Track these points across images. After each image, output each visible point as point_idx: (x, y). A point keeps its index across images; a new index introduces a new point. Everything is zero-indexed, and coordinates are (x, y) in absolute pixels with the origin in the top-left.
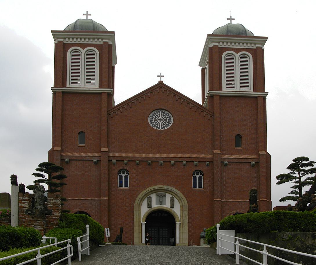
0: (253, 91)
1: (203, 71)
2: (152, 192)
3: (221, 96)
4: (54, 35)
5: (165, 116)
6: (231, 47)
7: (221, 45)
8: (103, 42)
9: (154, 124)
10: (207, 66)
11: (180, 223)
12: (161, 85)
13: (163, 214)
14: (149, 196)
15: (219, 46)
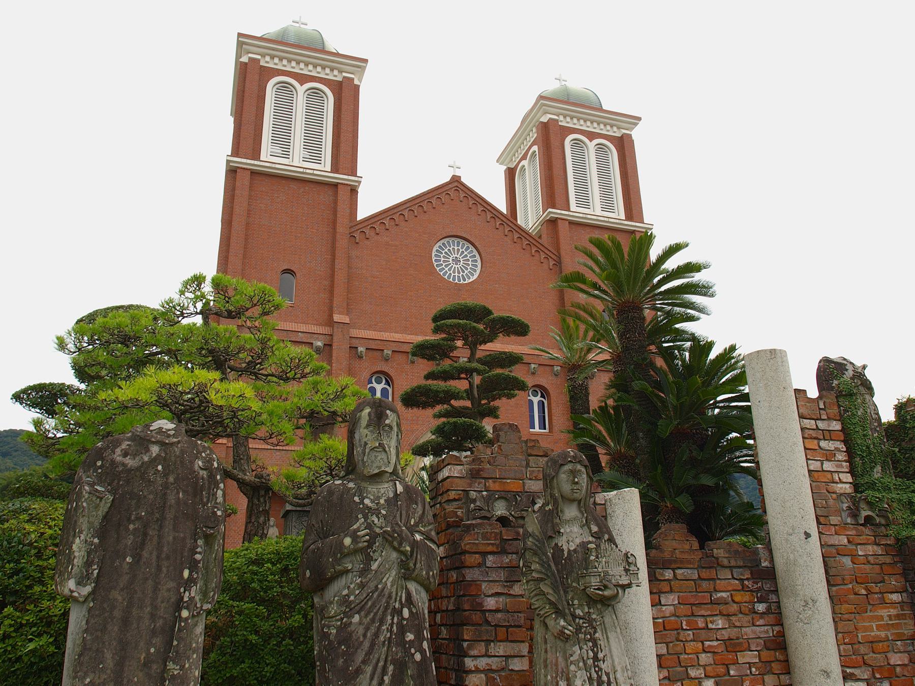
12: (456, 184)
15: (560, 124)
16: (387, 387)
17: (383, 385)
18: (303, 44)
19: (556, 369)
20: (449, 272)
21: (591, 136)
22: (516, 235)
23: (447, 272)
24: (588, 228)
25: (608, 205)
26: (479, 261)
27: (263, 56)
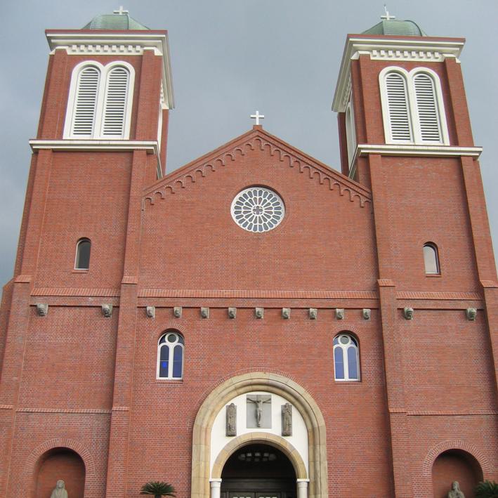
0: (449, 145)
1: (342, 118)
2: (238, 390)
3: (384, 156)
4: (49, 39)
5: (268, 201)
6: (394, 59)
7: (375, 56)
8: (145, 51)
9: (244, 220)
10: (350, 105)
11: (308, 480)
12: (257, 133)
13: (266, 455)
14: (229, 404)
15: (372, 58)
16: (180, 344)
17: (176, 343)
18: (109, 28)
19: (364, 312)
20: (250, 223)
21: (409, 66)
22: (323, 177)
23: (247, 223)
24: (406, 159)
25: (430, 132)
26: (283, 207)
27: (70, 46)
